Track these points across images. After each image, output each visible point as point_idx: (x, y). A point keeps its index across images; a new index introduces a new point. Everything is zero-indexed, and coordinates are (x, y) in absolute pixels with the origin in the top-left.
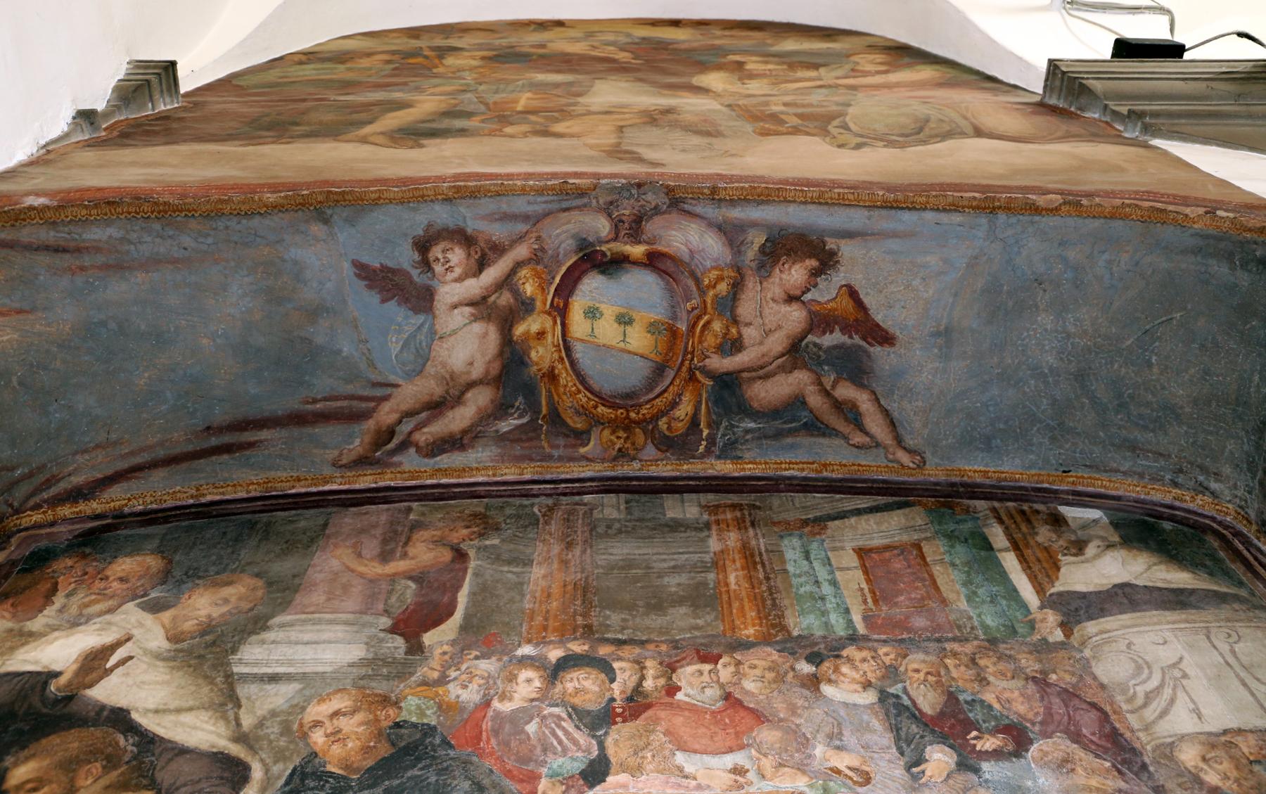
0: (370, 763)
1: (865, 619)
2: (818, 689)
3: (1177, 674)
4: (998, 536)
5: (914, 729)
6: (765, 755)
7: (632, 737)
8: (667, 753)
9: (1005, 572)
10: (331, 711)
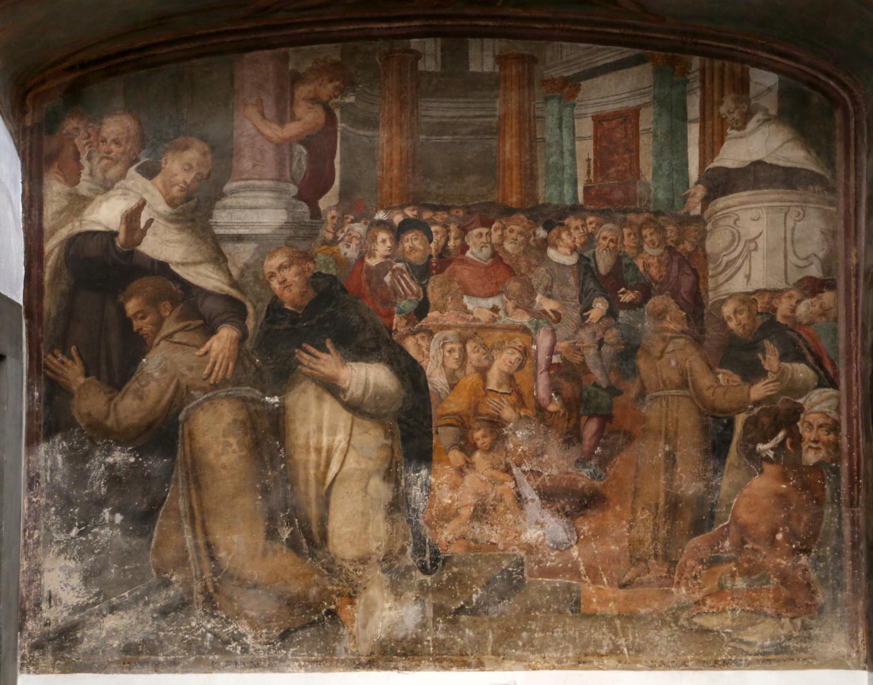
0: (306, 303)
1: (586, 190)
2: (545, 251)
3: (752, 246)
4: (694, 110)
5: (592, 285)
6: (510, 299)
7: (441, 285)
8: (459, 296)
9: (686, 145)
10: (278, 265)
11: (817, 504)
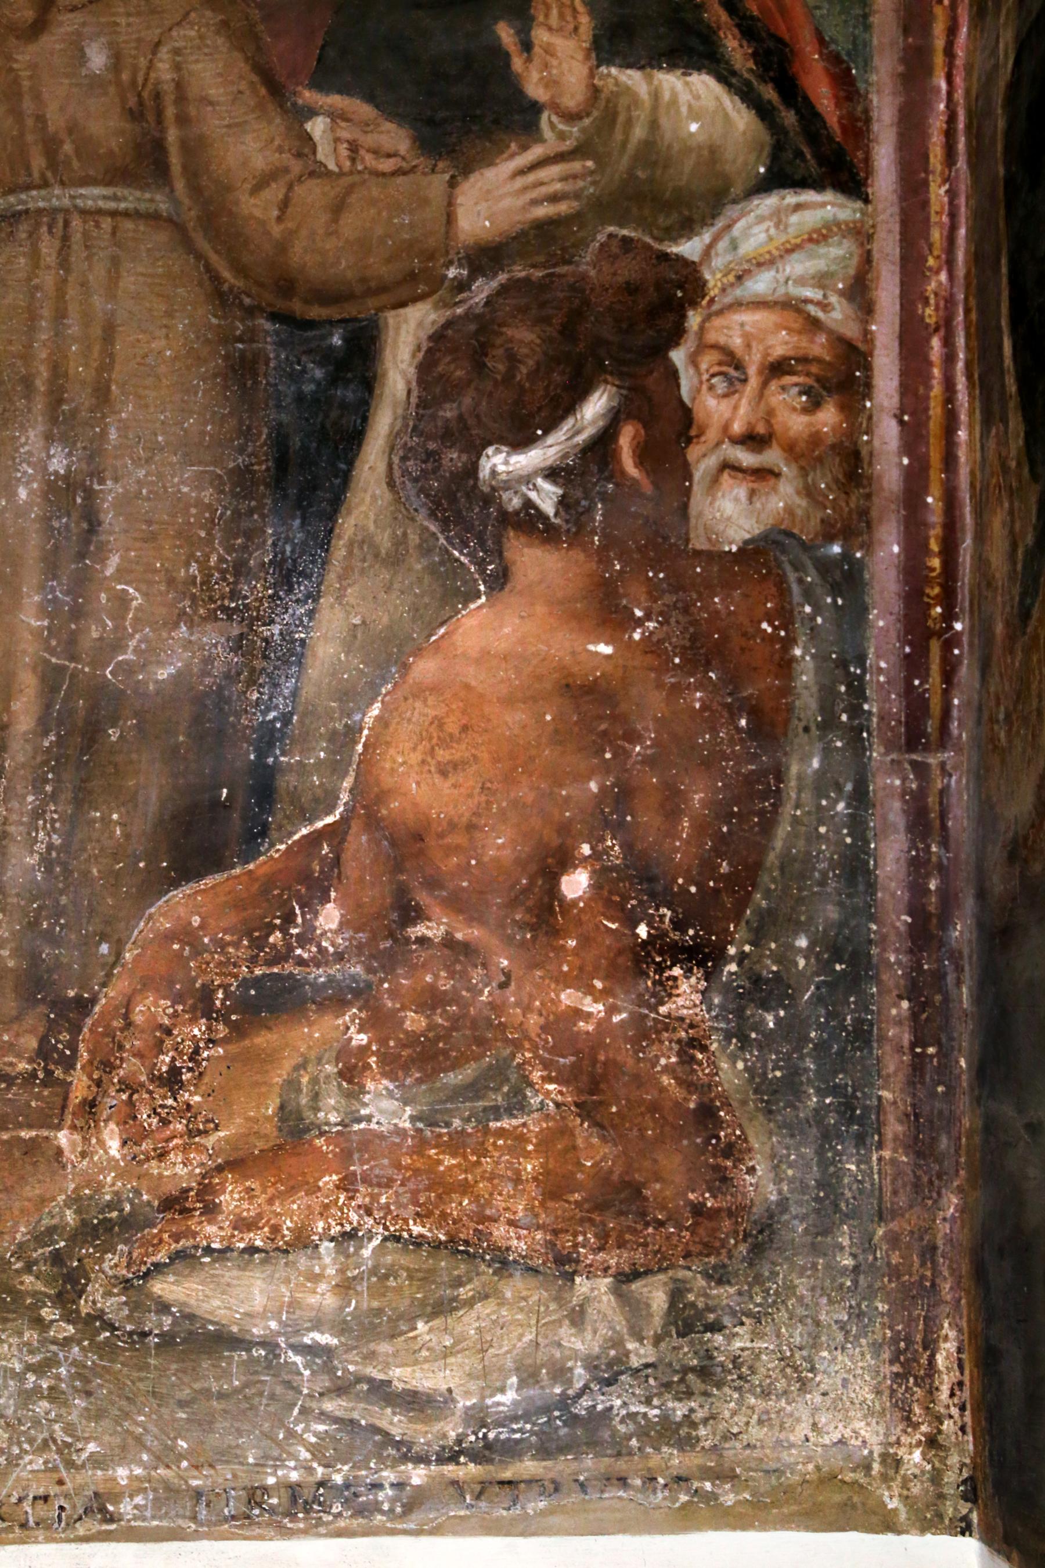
11: (755, 731)
